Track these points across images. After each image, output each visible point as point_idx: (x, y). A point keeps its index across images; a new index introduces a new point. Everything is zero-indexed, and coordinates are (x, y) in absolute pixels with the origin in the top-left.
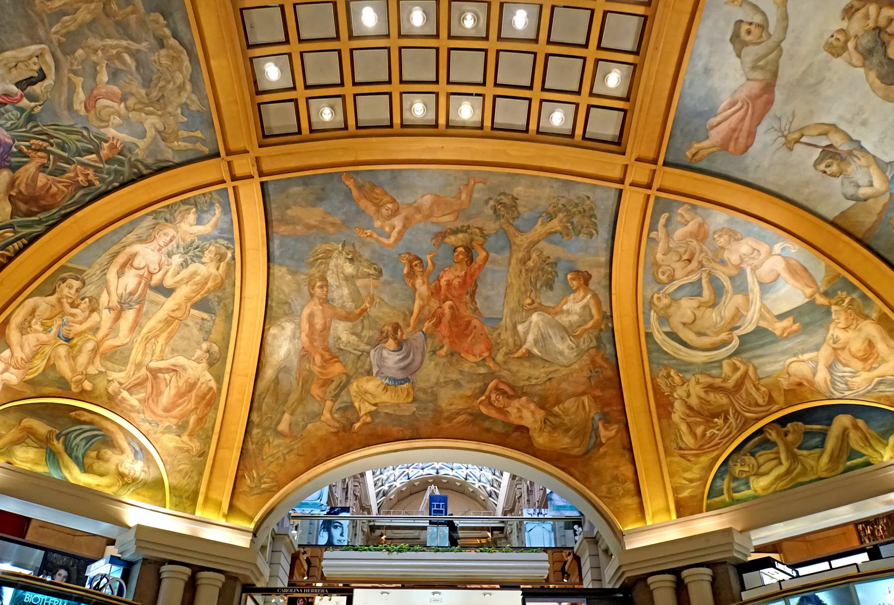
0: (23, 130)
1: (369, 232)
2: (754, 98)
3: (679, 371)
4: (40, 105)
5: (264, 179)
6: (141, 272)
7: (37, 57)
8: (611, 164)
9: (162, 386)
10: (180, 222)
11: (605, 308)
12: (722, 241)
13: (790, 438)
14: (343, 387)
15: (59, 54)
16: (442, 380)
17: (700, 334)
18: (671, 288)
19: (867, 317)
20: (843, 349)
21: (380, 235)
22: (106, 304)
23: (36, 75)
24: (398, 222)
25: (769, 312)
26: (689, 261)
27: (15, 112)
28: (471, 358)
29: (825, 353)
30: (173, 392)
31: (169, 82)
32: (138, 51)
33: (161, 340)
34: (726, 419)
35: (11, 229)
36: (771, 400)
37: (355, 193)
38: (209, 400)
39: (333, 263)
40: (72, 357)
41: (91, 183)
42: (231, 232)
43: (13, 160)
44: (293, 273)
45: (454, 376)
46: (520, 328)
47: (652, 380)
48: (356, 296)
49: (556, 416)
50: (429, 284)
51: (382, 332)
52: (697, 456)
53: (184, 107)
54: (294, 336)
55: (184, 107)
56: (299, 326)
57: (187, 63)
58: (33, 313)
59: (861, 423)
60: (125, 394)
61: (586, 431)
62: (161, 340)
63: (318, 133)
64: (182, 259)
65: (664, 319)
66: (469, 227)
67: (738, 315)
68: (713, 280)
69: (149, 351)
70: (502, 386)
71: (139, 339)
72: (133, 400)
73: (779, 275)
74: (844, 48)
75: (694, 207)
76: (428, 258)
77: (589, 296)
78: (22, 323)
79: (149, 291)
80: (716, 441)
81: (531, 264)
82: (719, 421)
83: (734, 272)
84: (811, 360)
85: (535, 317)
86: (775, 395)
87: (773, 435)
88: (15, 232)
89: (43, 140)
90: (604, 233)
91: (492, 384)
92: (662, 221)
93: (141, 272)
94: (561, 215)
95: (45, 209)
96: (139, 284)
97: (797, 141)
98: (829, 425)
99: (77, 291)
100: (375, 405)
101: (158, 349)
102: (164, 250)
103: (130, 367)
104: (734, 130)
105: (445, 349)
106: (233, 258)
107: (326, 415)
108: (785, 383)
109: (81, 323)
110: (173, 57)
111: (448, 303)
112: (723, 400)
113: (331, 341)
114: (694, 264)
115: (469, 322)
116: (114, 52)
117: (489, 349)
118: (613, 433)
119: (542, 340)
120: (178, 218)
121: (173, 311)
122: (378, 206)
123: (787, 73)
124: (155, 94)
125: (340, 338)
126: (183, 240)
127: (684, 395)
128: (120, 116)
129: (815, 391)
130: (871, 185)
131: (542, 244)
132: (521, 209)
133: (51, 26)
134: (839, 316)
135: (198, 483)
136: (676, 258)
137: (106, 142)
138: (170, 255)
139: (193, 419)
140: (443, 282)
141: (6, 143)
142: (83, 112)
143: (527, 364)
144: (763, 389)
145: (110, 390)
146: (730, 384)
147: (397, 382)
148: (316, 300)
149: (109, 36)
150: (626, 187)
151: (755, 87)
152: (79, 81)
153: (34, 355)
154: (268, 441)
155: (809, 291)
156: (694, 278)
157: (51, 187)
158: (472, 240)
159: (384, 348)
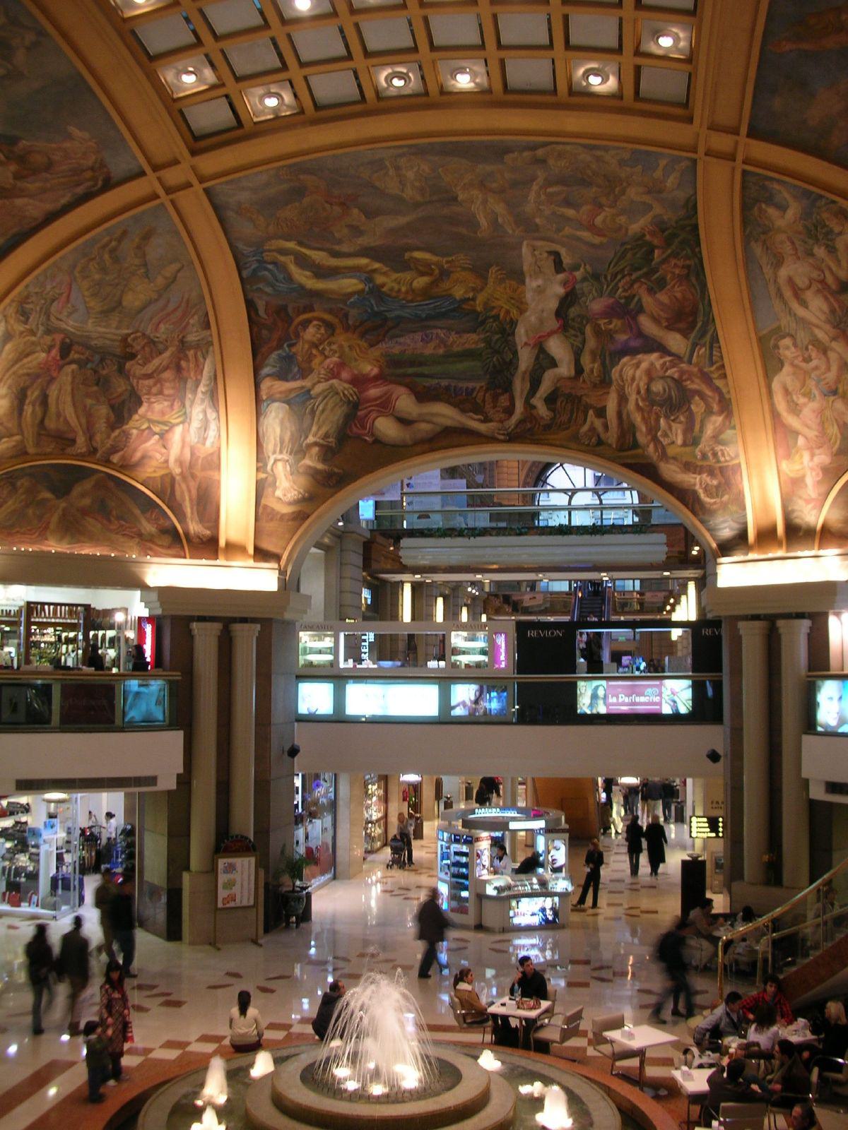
0: (605, 287)
4: (585, 265)
5: (744, 130)
7: (534, 250)
10: (773, 225)
23: (552, 257)
27: (585, 284)
35: (699, 347)
41: (688, 267)
43: (632, 306)
53: (622, 163)
55: (622, 163)
57: (568, 148)
58: (787, 392)
64: (823, 248)
88: (704, 345)
89: (623, 277)
95: (694, 313)
96: (826, 299)
99: (795, 345)
109: (828, 369)
116: (543, 197)
126: (800, 233)
137: (644, 235)
138: (812, 255)
142: (604, 240)
153: (822, 424)
157: (675, 297)
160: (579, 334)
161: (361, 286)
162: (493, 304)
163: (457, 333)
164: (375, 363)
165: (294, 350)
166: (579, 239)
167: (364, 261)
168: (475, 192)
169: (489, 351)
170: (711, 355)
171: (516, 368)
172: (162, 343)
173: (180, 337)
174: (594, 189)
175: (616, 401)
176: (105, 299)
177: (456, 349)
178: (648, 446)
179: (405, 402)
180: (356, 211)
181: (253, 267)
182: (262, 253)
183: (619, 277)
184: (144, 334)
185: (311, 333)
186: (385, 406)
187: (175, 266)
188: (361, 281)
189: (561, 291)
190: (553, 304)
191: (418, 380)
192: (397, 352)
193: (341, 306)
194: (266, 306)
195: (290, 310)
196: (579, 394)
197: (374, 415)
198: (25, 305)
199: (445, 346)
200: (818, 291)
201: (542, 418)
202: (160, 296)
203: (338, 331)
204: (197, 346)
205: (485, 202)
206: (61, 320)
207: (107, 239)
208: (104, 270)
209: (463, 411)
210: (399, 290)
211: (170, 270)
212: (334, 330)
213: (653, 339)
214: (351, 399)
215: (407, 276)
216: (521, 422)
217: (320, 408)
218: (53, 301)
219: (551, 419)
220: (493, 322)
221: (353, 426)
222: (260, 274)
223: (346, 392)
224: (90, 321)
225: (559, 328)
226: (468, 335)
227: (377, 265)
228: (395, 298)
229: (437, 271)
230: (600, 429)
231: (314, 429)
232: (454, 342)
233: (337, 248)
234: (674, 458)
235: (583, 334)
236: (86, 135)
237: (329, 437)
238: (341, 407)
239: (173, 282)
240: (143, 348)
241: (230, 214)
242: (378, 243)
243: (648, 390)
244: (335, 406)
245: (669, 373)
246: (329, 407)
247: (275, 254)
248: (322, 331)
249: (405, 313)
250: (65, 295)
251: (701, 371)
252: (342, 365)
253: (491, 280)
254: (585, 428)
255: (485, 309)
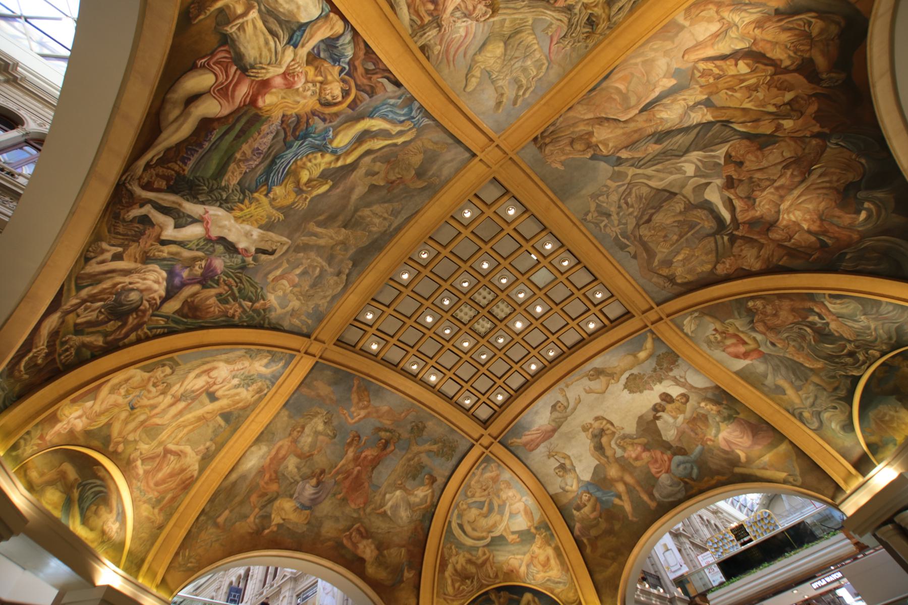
1: (345, 411)
2: (547, 432)
3: (457, 547)
6: (210, 380)
8: (475, 430)
9: (165, 465)
11: (435, 500)
12: (503, 486)
13: (502, 600)
14: (271, 501)
15: (292, 249)
16: (330, 514)
17: (474, 529)
18: (470, 501)
19: (550, 545)
20: (536, 558)
21: (349, 415)
22: (173, 392)
24: (363, 413)
25: (509, 528)
26: (485, 490)
27: (239, 261)
28: (353, 506)
29: (527, 558)
30: (169, 471)
31: (323, 291)
32: (326, 270)
33: (186, 430)
34: (472, 582)
36: (497, 576)
37: (355, 388)
38: (187, 485)
39: (315, 420)
40: (126, 422)
41: (233, 316)
42: (277, 379)
43: (210, 282)
44: (290, 417)
45: (338, 514)
46: (388, 496)
47: (442, 549)
48: (313, 445)
49: (384, 556)
50: (355, 453)
51: (313, 472)
52: (453, 600)
53: (317, 306)
54: (263, 457)
55: (317, 306)
56: (269, 451)
57: (340, 289)
59: (536, 600)
60: (139, 463)
61: (397, 571)
62: (186, 430)
63: (366, 353)
65: (460, 516)
66: (395, 431)
67: (495, 525)
68: (491, 504)
69: (173, 435)
70: (362, 529)
71: (174, 424)
72: (141, 468)
73: (519, 512)
74: (588, 430)
75: (499, 465)
76: (364, 439)
77: (430, 491)
78: (116, 385)
79: (204, 395)
80: (464, 593)
81: (412, 462)
82: (468, 582)
83: (501, 502)
84: (520, 559)
85: (398, 493)
86: (499, 574)
87: (493, 597)
88: (166, 323)
89: (235, 282)
90: (454, 461)
91: (356, 526)
92: (483, 466)
93: (210, 380)
94: (440, 444)
97: (553, 456)
98: (522, 596)
99: (165, 376)
100: (284, 520)
101: (180, 436)
102: (234, 373)
103: (155, 443)
104: (532, 440)
105: (342, 495)
106: (266, 395)
107: (252, 519)
108: (505, 568)
109: (149, 399)
110: (337, 283)
111: (359, 468)
112: (472, 569)
113: (282, 467)
114: (486, 493)
115: (363, 483)
116: (315, 264)
117: (365, 504)
118: (411, 575)
119: (395, 507)
120: (257, 359)
121: (208, 413)
122: (360, 400)
123: (564, 429)
124: (311, 292)
125: (287, 467)
127: (455, 562)
128: (284, 293)
129: (518, 577)
130: (572, 486)
131: (423, 456)
132: (424, 433)
133: (304, 236)
134: (538, 540)
135: (148, 552)
136: (480, 487)
137: (264, 300)
138: (234, 377)
139: (169, 496)
140: (363, 455)
141: (216, 272)
143: (381, 519)
144: (494, 569)
145: (132, 457)
146: (480, 561)
147: (304, 507)
148: (290, 438)
149: (321, 257)
150: (477, 444)
151: (549, 428)
152: (285, 265)
153: (107, 410)
154: (207, 528)
155: (529, 524)
156: (483, 499)
158: (392, 438)
159: (308, 482)
160: (198, 247)
161: (335, 144)
162: (254, 204)
163: (246, 172)
164: (268, 108)
165: (337, 69)
166: (276, 268)
167: (349, 160)
168: (341, 238)
169: (215, 186)
170: (159, 328)
171: (188, 200)
172: (458, 18)
173: (443, 30)
174: (307, 288)
175: (126, 267)
176: (519, 44)
177: (232, 166)
178: (77, 299)
179: (211, 108)
180: (382, 184)
181: (414, 114)
182: (414, 125)
183: (237, 280)
184: (477, 21)
185: (335, 90)
186: (223, 91)
187: (469, 89)
188: (337, 148)
189: (241, 245)
190: (231, 238)
191: (224, 128)
192: (263, 128)
193: (333, 124)
194: (385, 89)
195: (366, 96)
196: (140, 241)
197: (222, 78)
198: (590, 30)
199: (240, 160)
200: (208, 383)
201: (128, 212)
202: (473, 60)
203: (318, 107)
204: (423, 27)
205: (332, 238)
206: (558, 20)
207: (527, 95)
208: (524, 70)
209: (168, 150)
210: (310, 161)
211: (474, 82)
212: (322, 104)
213: (176, 294)
214: (254, 70)
215: (316, 173)
216: (131, 194)
217: (272, 43)
218: (564, 36)
219: (124, 219)
220: (239, 199)
221: (227, 55)
222: (406, 110)
223: (263, 71)
224: (530, 22)
225: (209, 236)
226: (238, 179)
227: (340, 164)
228: (307, 156)
229: (305, 188)
230: (100, 258)
231: (260, 24)
232: (239, 167)
233: (372, 156)
234: (63, 322)
235: (197, 250)
236: (555, 165)
237: (239, 29)
238: (255, 59)
239: (467, 75)
240: (475, 8)
241: (450, 141)
242: (353, 176)
243: (133, 290)
244: (261, 55)
245: (145, 303)
246: (265, 52)
247: (406, 129)
248: (329, 97)
249: (289, 154)
250: (554, 42)
251: (145, 323)
252: (289, 86)
253: (274, 212)
254: (105, 245)
255: (253, 198)
